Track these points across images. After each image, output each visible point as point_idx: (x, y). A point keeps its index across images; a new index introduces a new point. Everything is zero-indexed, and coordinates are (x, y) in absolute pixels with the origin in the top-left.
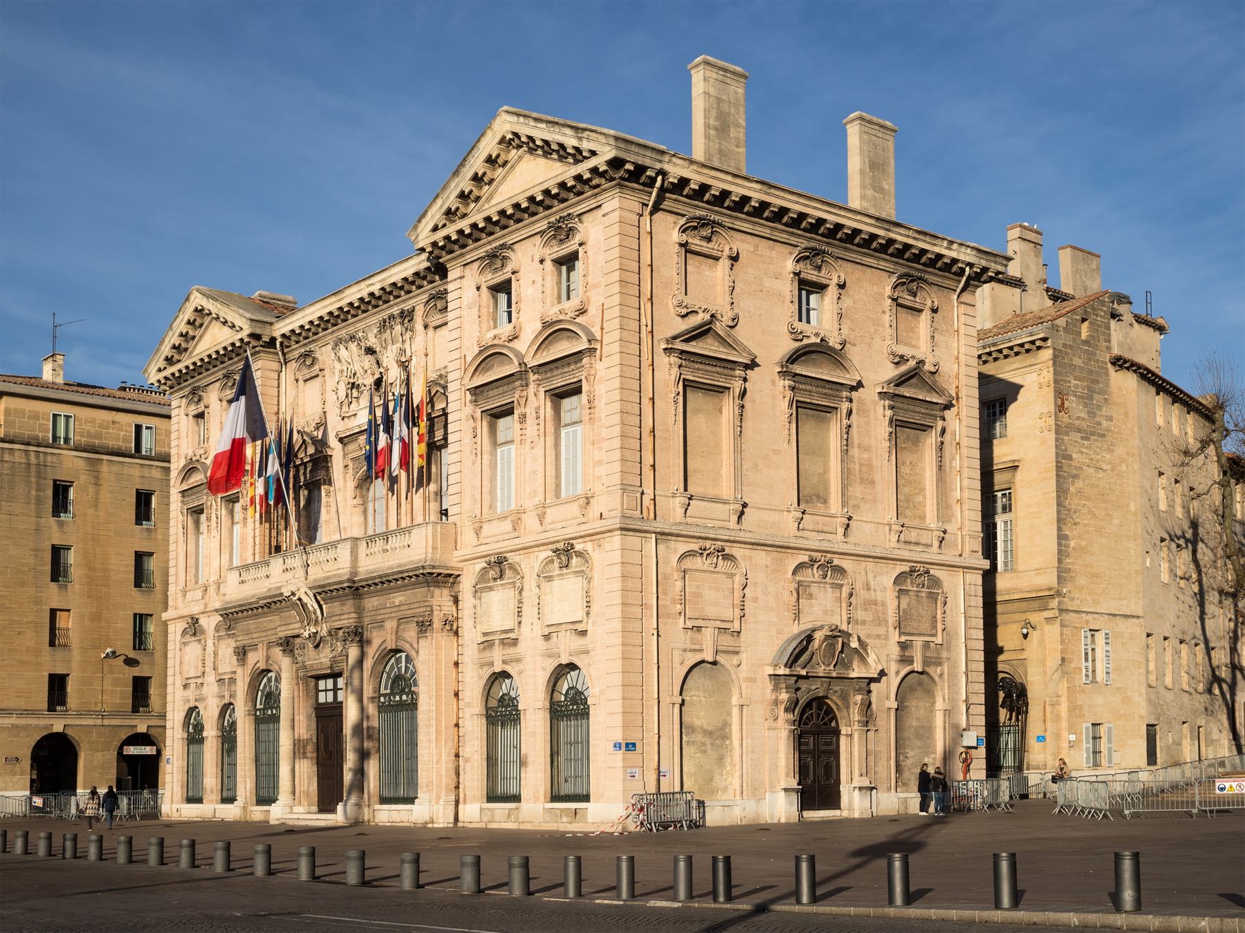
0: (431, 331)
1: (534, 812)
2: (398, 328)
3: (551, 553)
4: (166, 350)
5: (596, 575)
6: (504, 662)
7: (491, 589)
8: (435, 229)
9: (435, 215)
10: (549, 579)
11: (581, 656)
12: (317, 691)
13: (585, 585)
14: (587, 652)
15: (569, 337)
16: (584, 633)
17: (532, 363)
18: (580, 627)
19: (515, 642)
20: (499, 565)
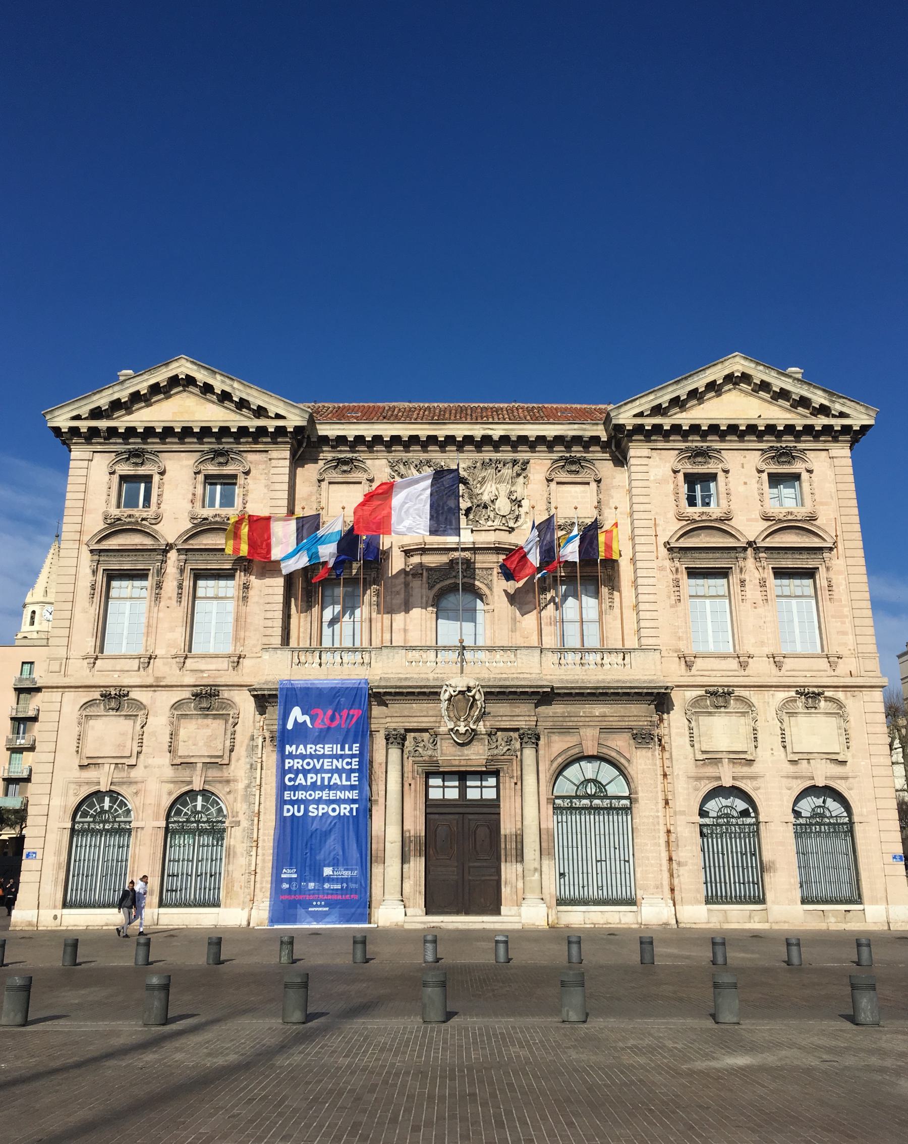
0: (553, 485)
1: (785, 909)
2: (507, 472)
3: (793, 694)
4: (102, 400)
5: (851, 718)
6: (734, 778)
7: (710, 714)
8: (640, 415)
9: (645, 403)
10: (791, 714)
11: (839, 781)
12: (427, 787)
13: (843, 725)
14: (846, 778)
15: (797, 534)
16: (844, 763)
17: (760, 544)
18: (841, 758)
19: (750, 762)
20: (719, 697)
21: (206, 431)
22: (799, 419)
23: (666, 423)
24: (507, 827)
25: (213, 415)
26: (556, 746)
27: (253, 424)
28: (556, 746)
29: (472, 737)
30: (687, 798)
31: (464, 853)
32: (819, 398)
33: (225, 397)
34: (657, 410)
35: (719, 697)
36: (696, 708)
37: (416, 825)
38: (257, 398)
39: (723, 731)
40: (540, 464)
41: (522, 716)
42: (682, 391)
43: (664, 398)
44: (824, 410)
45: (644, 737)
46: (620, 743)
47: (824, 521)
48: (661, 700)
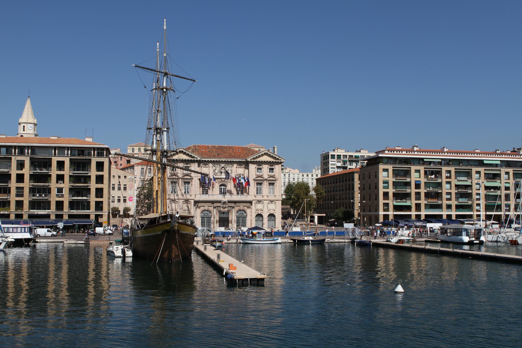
20: (259, 201)
21: (185, 160)
22: (274, 161)
23: (255, 160)
24: (230, 219)
25: (187, 158)
26: (237, 208)
27: (192, 159)
28: (237, 208)
29: (226, 207)
30: (254, 215)
31: (224, 221)
32: (277, 157)
33: (188, 155)
34: (254, 158)
35: (259, 201)
36: (256, 203)
37: (218, 219)
38: (193, 155)
39: (259, 206)
40: (235, 165)
41: (233, 205)
42: (257, 155)
43: (255, 157)
44: (278, 159)
45: (248, 207)
46: (245, 208)
47: (277, 176)
48: (251, 202)
